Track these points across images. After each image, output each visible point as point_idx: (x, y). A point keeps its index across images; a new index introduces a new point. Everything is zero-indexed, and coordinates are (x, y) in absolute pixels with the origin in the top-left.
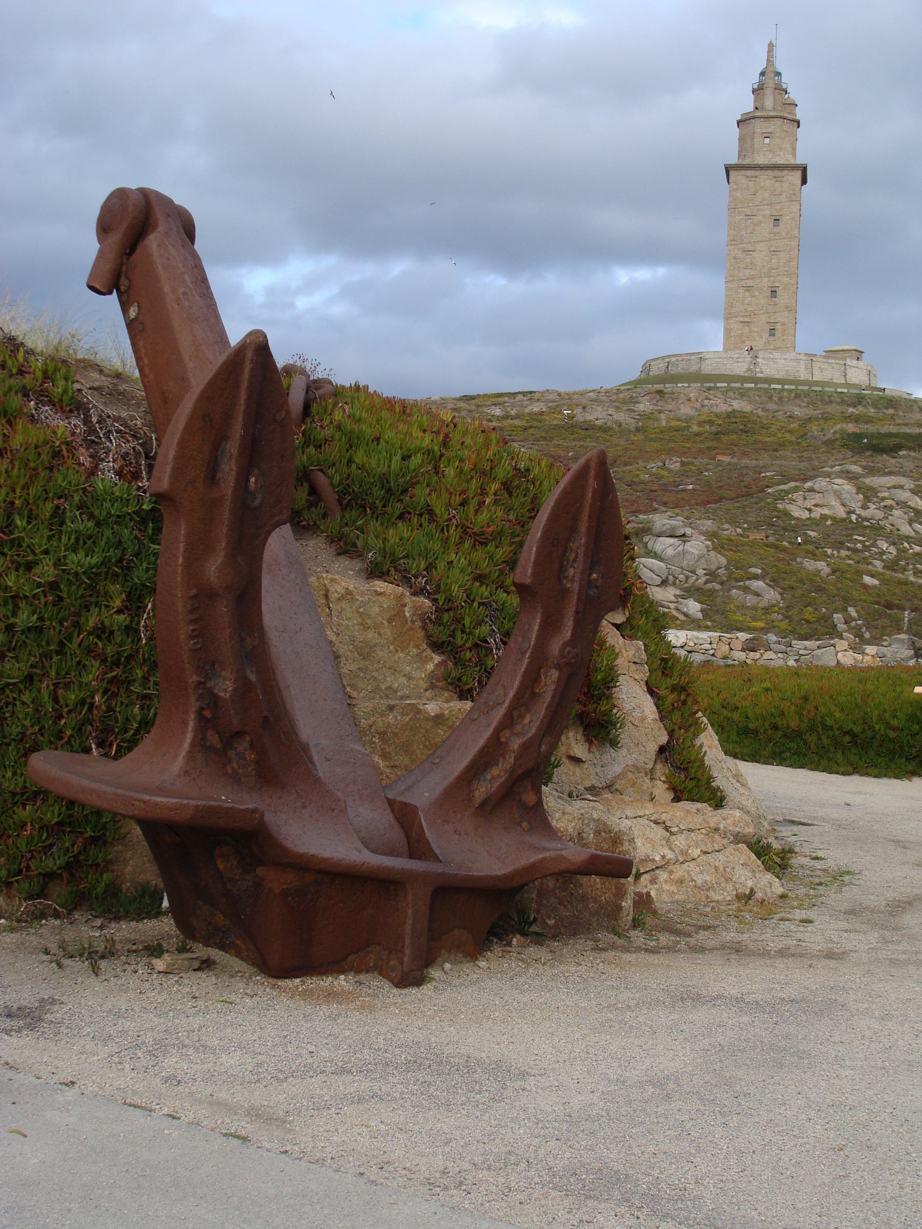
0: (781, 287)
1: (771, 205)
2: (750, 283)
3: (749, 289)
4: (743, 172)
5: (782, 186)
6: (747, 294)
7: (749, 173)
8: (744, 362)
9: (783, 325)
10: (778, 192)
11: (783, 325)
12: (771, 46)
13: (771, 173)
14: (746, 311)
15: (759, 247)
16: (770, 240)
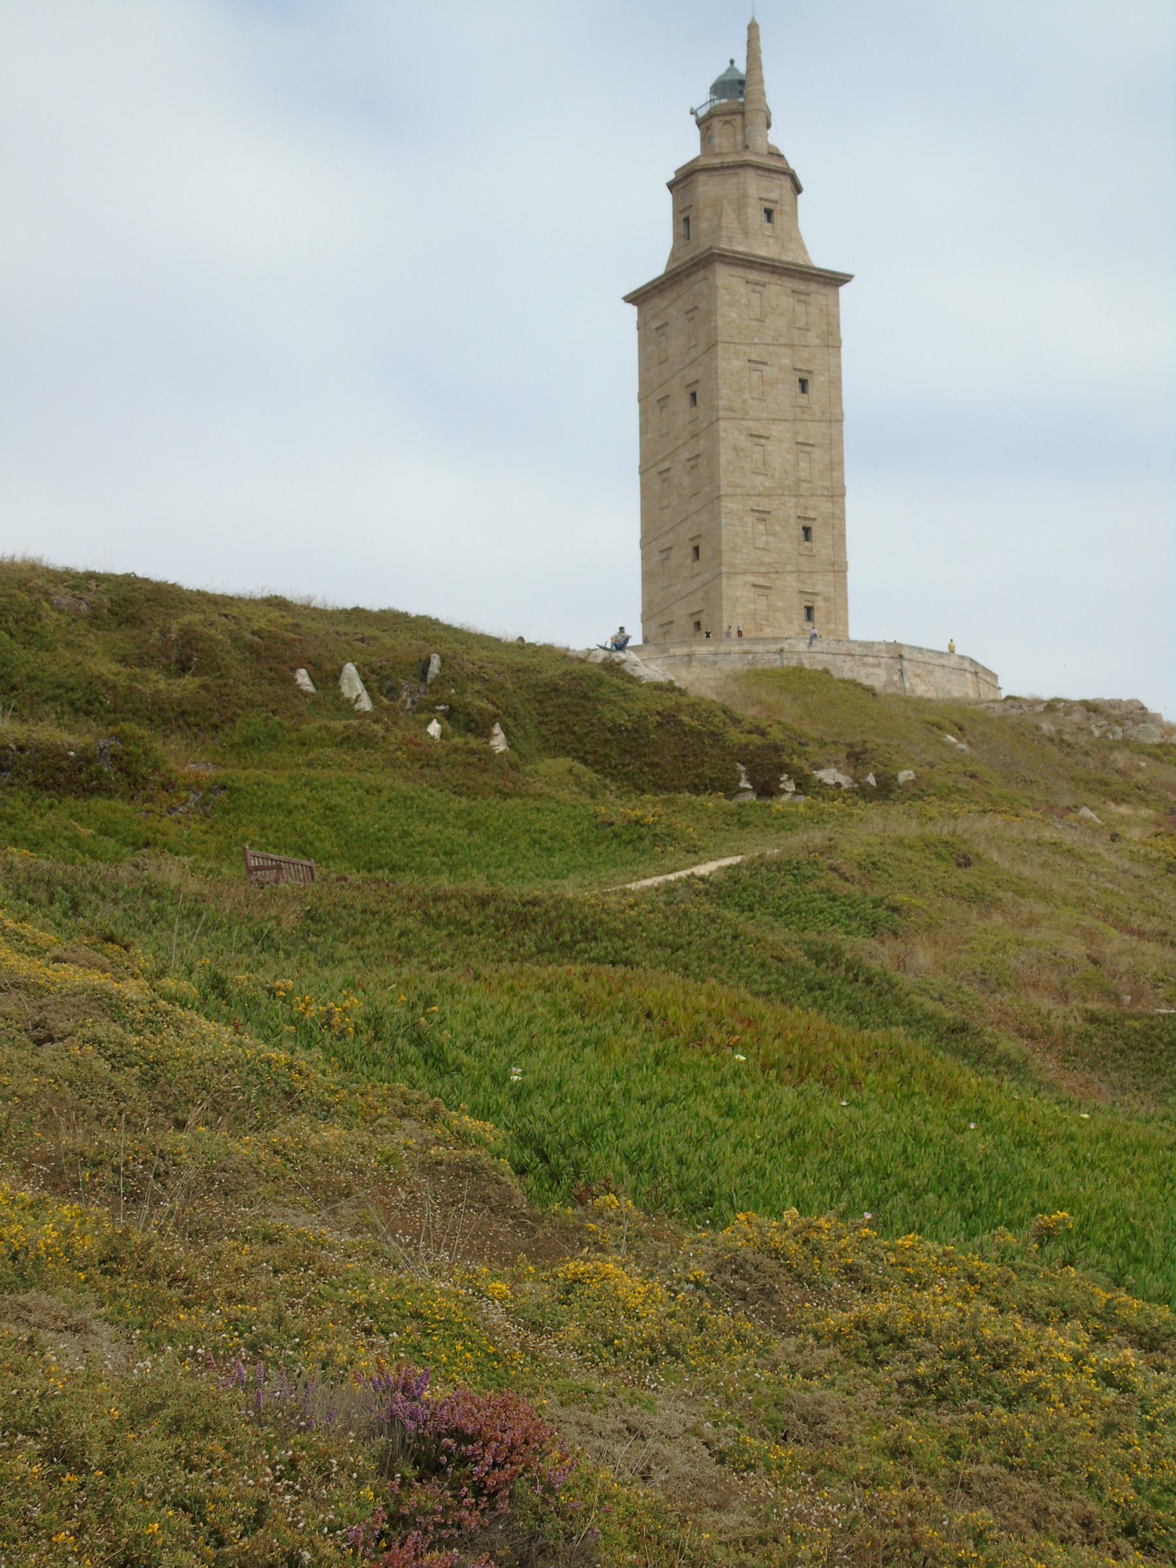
0: (820, 520)
1: (791, 346)
2: (764, 504)
3: (762, 515)
4: (740, 272)
5: (807, 313)
6: (761, 527)
7: (753, 276)
8: (878, 666)
9: (827, 600)
10: (801, 323)
11: (827, 600)
12: (753, 28)
13: (790, 284)
14: (762, 564)
15: (776, 430)
16: (795, 420)
